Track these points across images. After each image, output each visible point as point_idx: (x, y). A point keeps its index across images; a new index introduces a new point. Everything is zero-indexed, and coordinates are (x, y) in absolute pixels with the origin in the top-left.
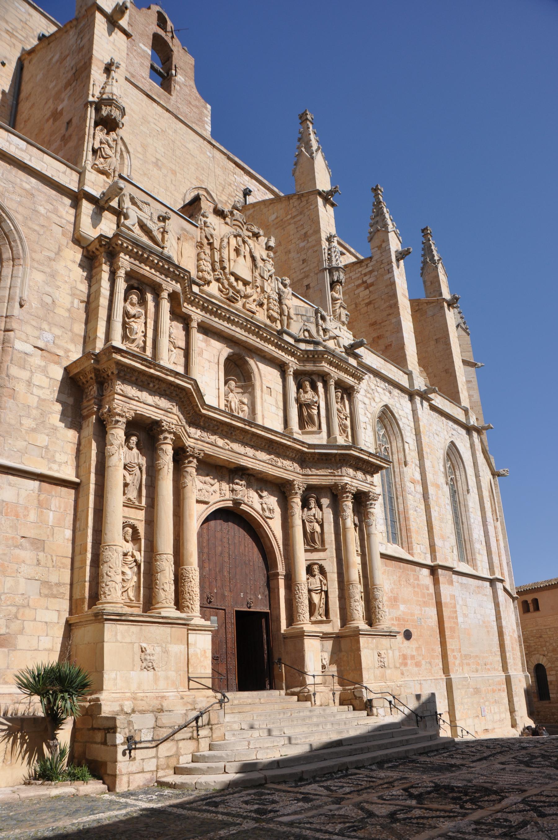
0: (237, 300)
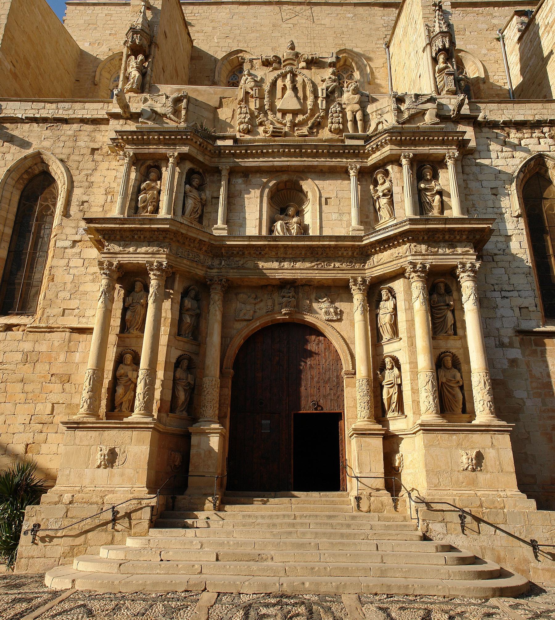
0: (281, 132)
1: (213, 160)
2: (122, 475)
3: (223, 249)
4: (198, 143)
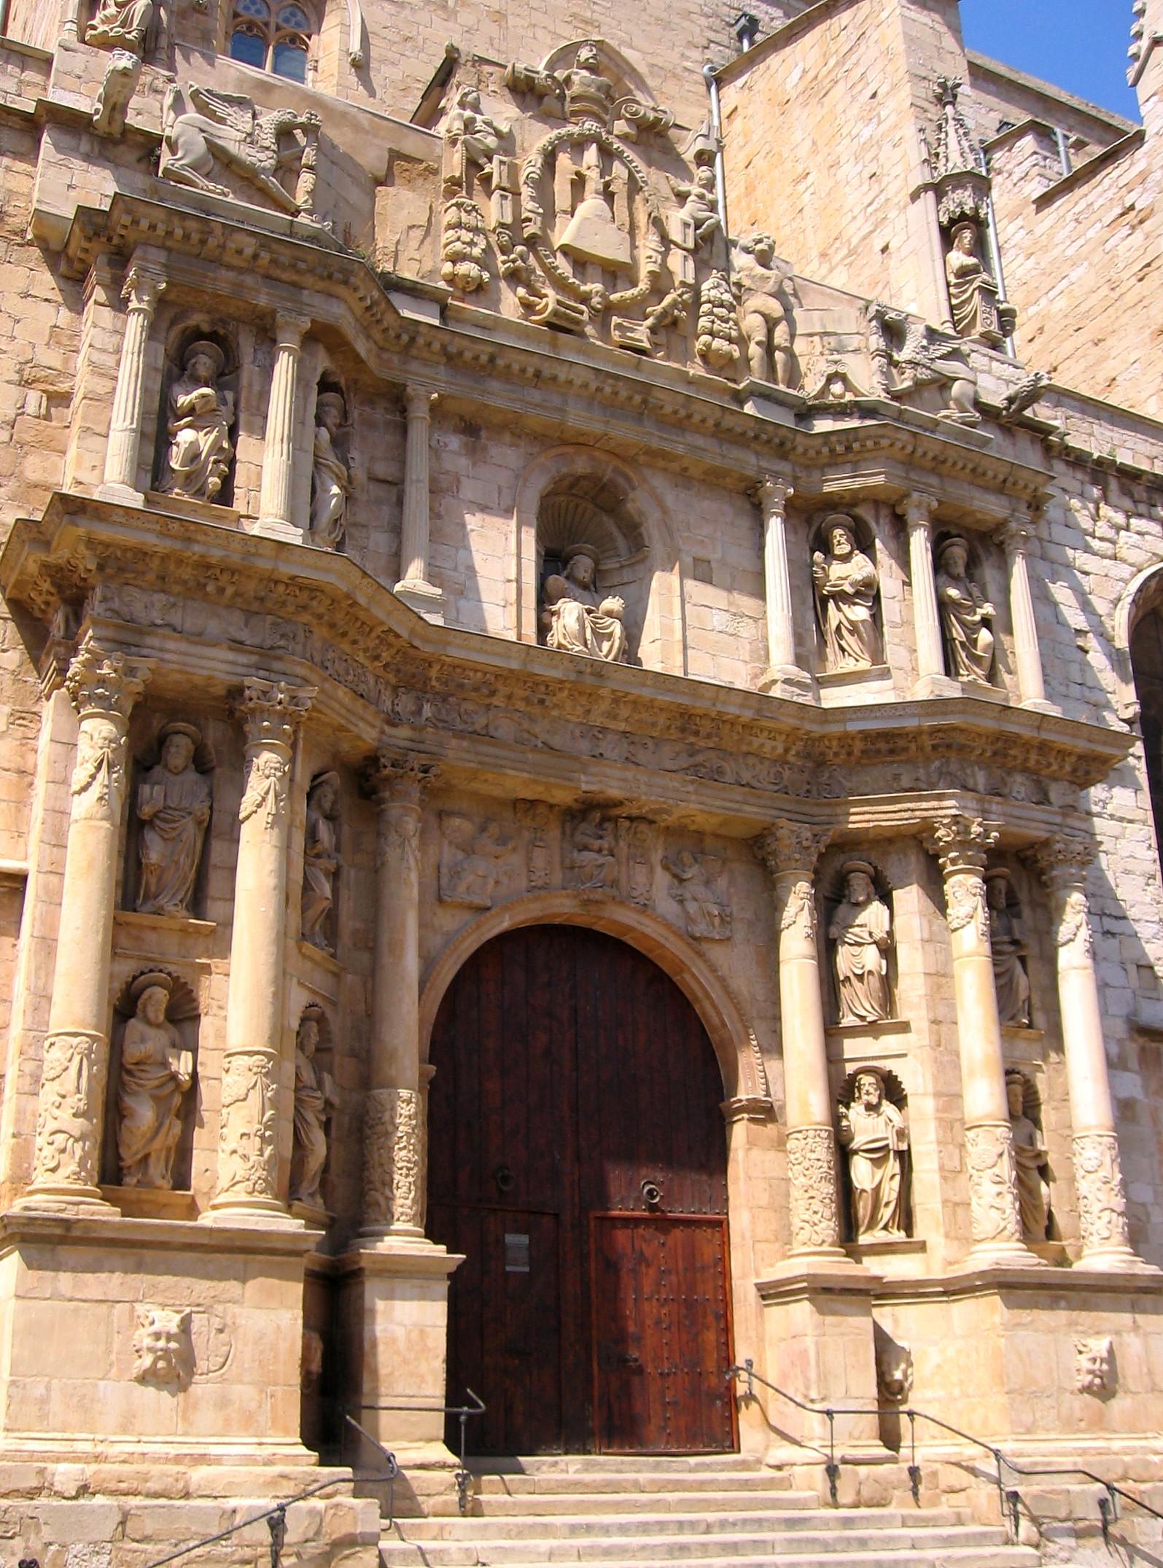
0: (578, 322)
1: (385, 356)
3: (436, 667)
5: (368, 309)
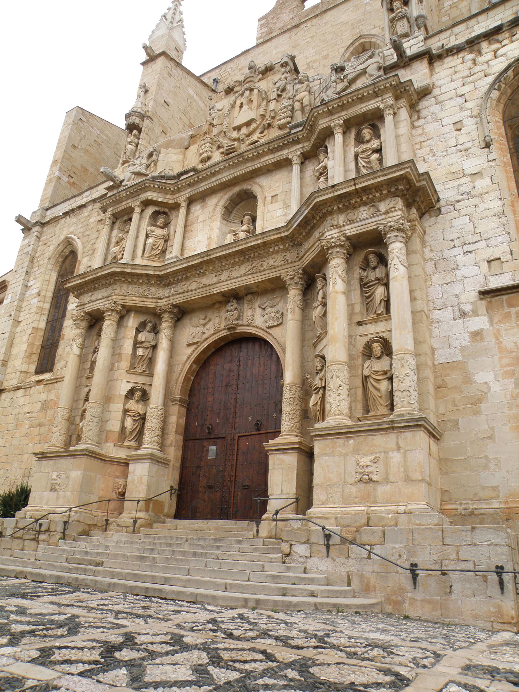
0: (234, 148)
2: (65, 497)
4: (156, 186)
5: (159, 187)
